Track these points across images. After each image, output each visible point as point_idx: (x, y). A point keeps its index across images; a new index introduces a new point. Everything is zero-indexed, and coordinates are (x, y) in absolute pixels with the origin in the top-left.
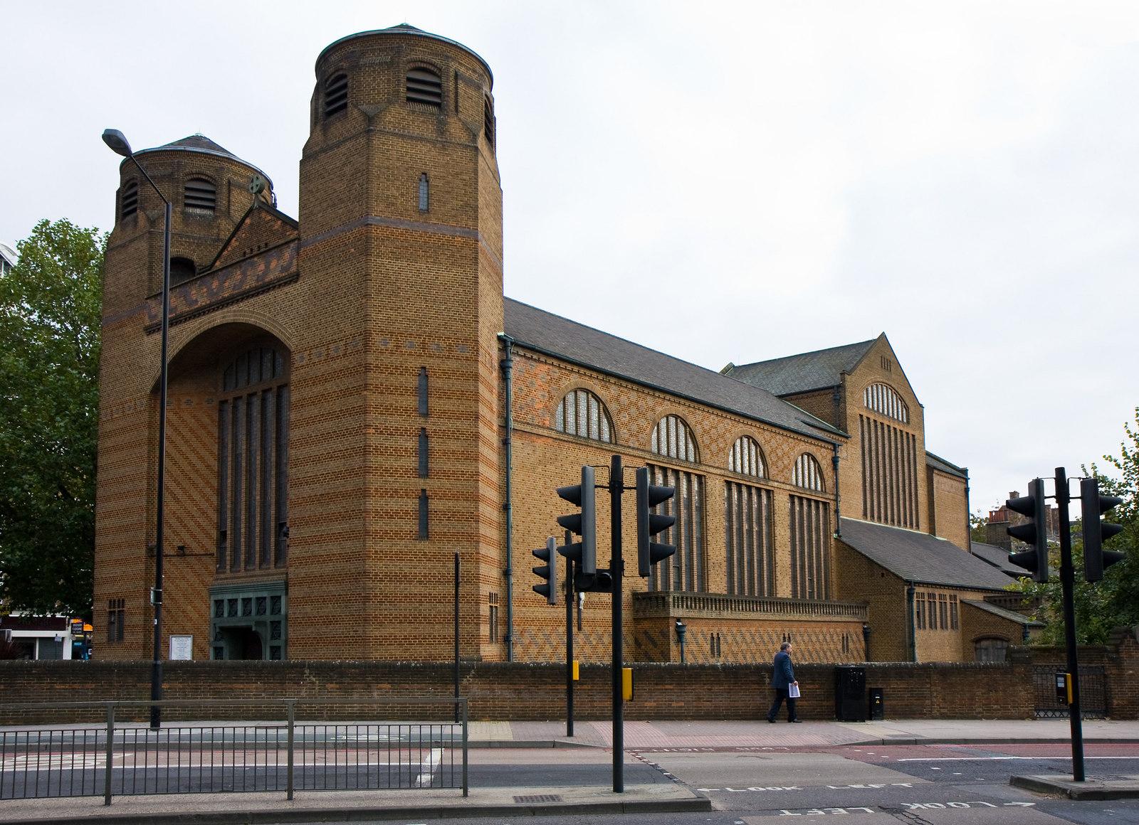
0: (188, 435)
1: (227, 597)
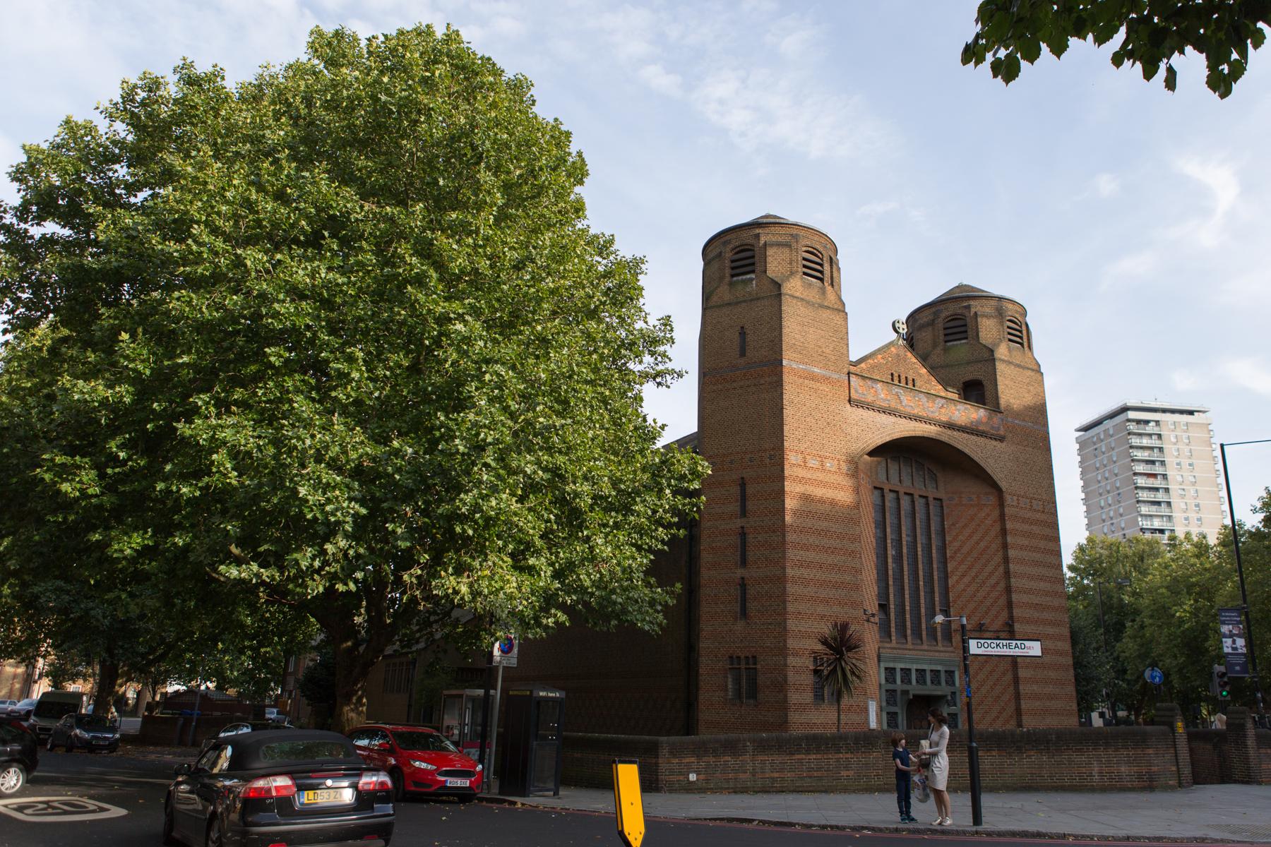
1: (899, 666)
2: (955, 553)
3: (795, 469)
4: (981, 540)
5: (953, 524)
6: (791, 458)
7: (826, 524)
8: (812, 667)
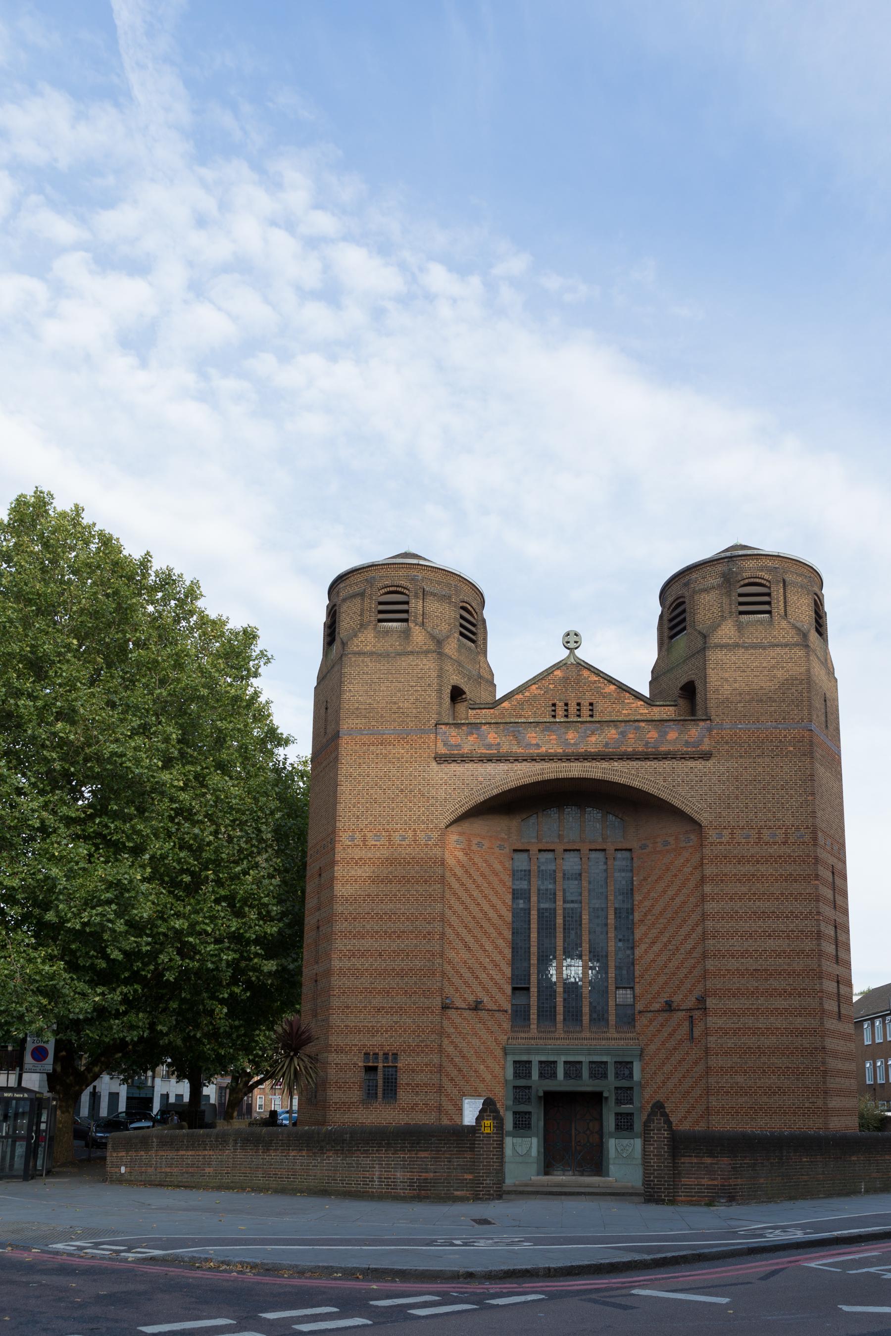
0: (480, 880)
2: (646, 915)
3: (349, 851)
4: (676, 895)
5: (645, 879)
6: (344, 838)
7: (391, 906)
8: (361, 1064)
